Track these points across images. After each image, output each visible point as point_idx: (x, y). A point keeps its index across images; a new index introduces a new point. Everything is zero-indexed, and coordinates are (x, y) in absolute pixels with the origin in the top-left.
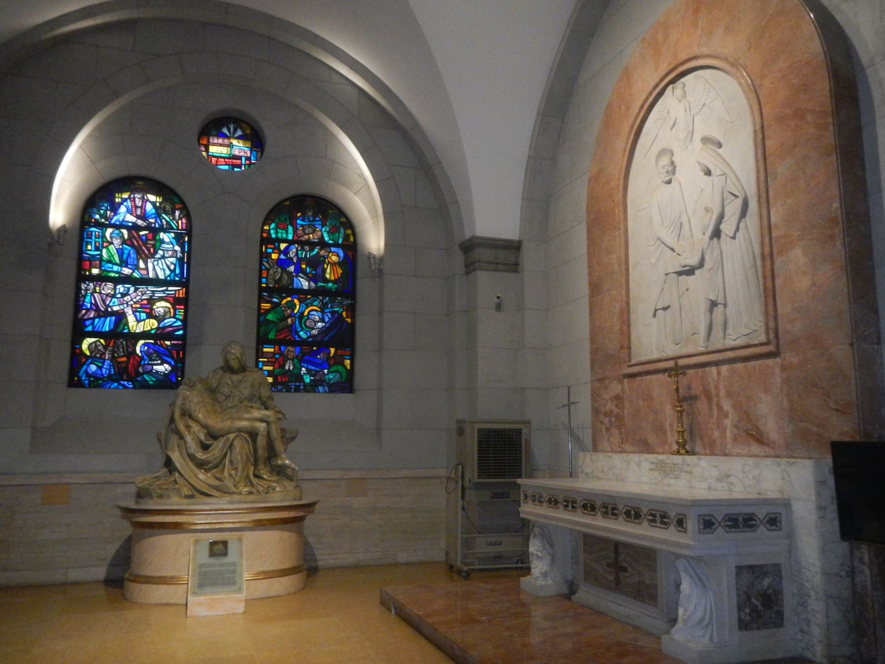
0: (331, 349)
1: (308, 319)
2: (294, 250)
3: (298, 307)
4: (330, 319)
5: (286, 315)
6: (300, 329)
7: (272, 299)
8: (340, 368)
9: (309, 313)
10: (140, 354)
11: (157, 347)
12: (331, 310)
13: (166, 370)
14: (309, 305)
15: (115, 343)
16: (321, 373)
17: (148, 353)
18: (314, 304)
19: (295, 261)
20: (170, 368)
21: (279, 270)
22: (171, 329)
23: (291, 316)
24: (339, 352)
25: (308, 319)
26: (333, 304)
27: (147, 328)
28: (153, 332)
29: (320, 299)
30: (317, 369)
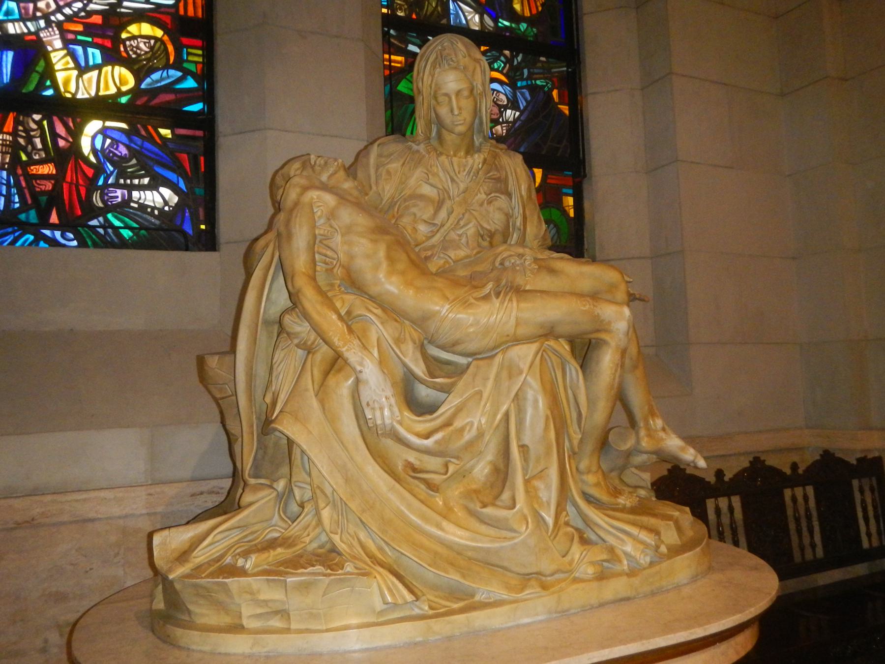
7: (407, 46)
8: (555, 214)
10: (92, 159)
11: (139, 141)
12: (529, 82)
13: (166, 203)
15: (17, 122)
17: (115, 154)
18: (496, 66)
20: (176, 199)
22: (171, 97)
24: (553, 180)
27: (107, 88)
28: (124, 100)
29: (505, 56)
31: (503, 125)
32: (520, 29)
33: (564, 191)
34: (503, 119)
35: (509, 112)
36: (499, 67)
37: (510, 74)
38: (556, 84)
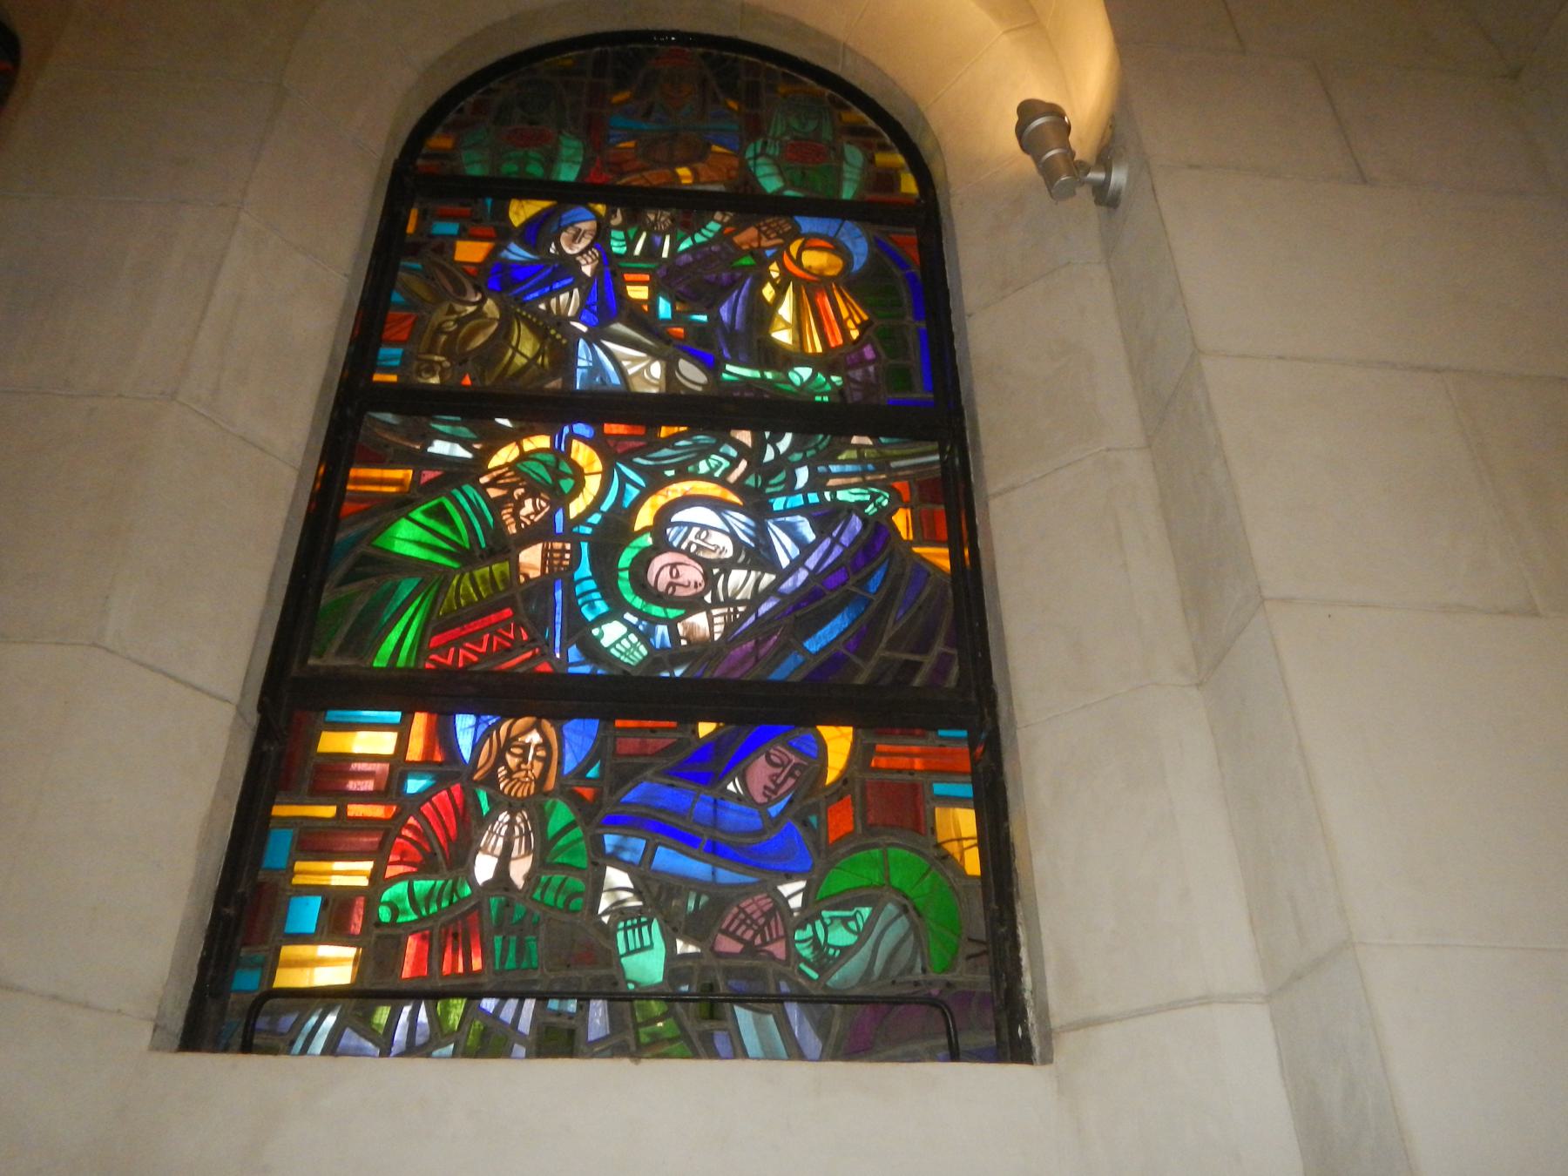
0: (827, 732)
1: (661, 545)
2: (587, 226)
3: (593, 484)
4: (806, 549)
5: (513, 530)
6: (602, 607)
8: (904, 866)
9: (664, 517)
12: (813, 498)
14: (670, 473)
16: (755, 905)
18: (703, 467)
19: (587, 270)
21: (490, 307)
23: (539, 532)
25: (662, 545)
26: (821, 469)
29: (738, 445)
30: (726, 876)
31: (715, 612)
32: (790, 382)
33: (939, 789)
34: (715, 597)
35: (737, 576)
36: (712, 471)
37: (751, 481)
38: (906, 496)
